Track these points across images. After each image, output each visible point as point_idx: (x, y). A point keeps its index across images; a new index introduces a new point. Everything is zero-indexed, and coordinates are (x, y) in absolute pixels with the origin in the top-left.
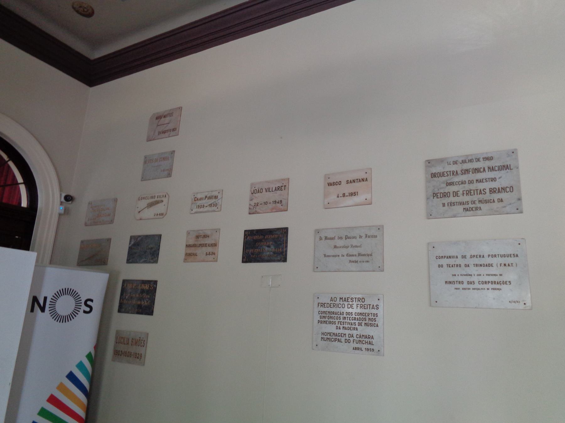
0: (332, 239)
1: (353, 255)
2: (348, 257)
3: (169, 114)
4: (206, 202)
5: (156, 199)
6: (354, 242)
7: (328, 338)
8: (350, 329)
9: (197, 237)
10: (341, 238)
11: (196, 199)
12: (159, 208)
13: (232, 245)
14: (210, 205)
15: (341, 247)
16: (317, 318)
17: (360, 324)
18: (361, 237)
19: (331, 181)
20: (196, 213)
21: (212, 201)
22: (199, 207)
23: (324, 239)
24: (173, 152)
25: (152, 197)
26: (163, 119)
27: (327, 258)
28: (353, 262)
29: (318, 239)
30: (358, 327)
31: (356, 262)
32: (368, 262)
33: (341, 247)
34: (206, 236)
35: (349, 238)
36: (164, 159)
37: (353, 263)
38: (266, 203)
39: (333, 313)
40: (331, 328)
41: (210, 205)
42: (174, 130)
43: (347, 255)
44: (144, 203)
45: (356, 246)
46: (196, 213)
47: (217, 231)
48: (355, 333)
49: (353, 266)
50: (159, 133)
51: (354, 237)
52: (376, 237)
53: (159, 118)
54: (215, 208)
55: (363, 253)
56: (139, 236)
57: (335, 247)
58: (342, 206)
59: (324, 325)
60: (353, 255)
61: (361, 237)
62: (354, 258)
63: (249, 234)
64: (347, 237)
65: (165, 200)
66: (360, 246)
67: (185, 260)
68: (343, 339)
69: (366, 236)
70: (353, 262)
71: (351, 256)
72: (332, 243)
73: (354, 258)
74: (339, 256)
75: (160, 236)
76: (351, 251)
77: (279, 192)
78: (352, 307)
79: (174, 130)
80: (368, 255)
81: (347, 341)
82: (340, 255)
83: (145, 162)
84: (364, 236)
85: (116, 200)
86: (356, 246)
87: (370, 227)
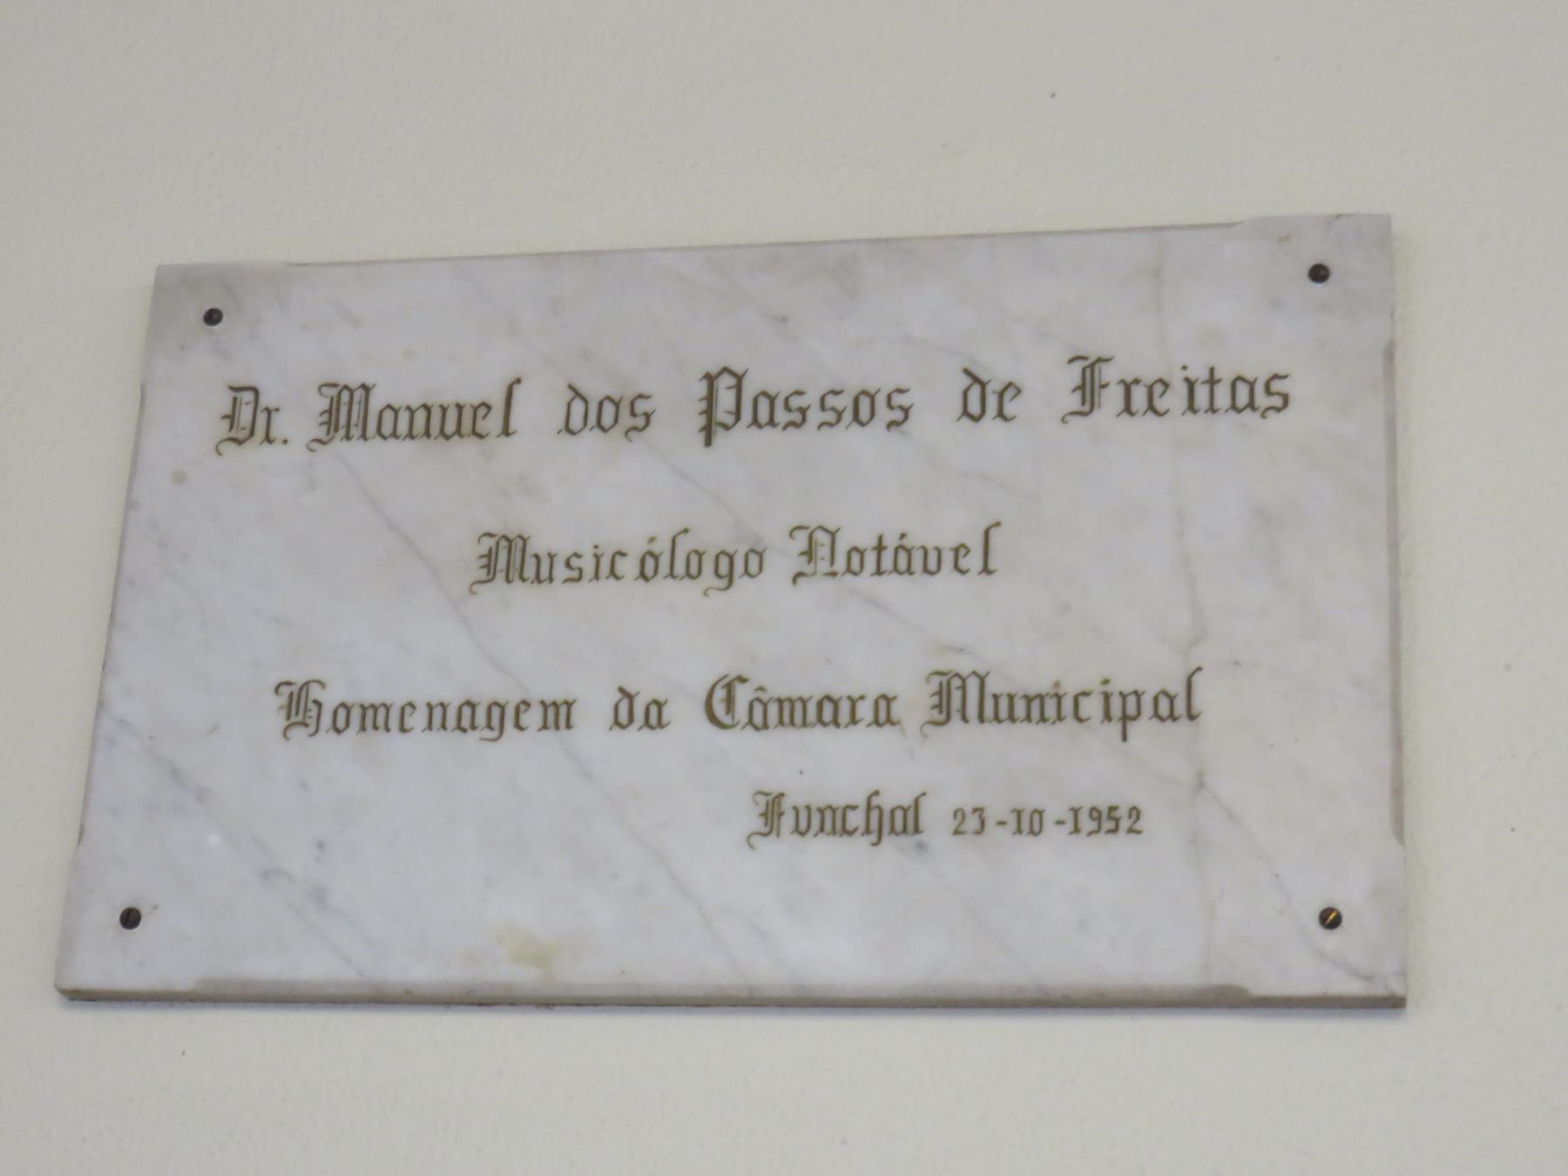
0: (452, 422)
1: (831, 712)
2: (740, 743)
6: (864, 480)
10: (619, 414)
15: (607, 566)
18: (985, 398)
23: (299, 420)
27: (334, 755)
28: (830, 821)
29: (193, 416)
31: (896, 822)
32: (1109, 820)
33: (607, 566)
35: (778, 411)
37: (824, 852)
43: (723, 703)
45: (901, 557)
49: (835, 909)
51: (861, 408)
52: (1261, 396)
55: (1024, 668)
57: (508, 559)
60: (831, 712)
61: (985, 398)
62: (840, 764)
64: (726, 404)
66: (978, 556)
69: (1089, 390)
70: (830, 821)
71: (791, 712)
72: (452, 494)
73: (840, 764)
74: (559, 714)
76: (795, 630)
80: (1123, 711)
82: (595, 706)
84: (1049, 384)
86: (901, 557)
87: (1160, 255)
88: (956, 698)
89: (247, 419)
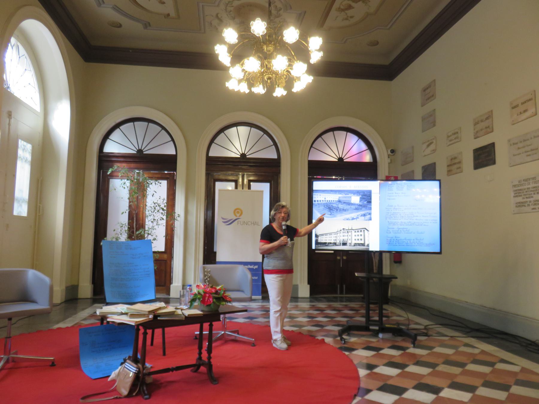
0: (517, 143)
3: (429, 86)
4: (453, 137)
6: (528, 143)
7: (520, 205)
8: (529, 198)
9: (452, 159)
10: (521, 142)
11: (448, 137)
12: (432, 147)
13: (468, 160)
14: (455, 139)
16: (512, 194)
17: (534, 194)
19: (514, 105)
20: (449, 145)
21: (456, 135)
22: (450, 141)
30: (534, 196)
34: (455, 158)
36: (431, 116)
38: (482, 130)
39: (520, 190)
40: (520, 199)
41: (455, 139)
42: (433, 96)
44: (425, 146)
45: (530, 145)
46: (449, 145)
47: (461, 153)
48: (532, 199)
49: (529, 159)
50: (427, 100)
51: (528, 140)
53: (425, 90)
54: (457, 140)
56: (425, 166)
58: (520, 120)
59: (516, 198)
61: (531, 138)
62: (528, 153)
63: (476, 151)
64: (525, 141)
65: (434, 141)
67: (448, 175)
68: (526, 205)
73: (528, 153)
75: (435, 163)
77: (487, 121)
78: (529, 184)
79: (433, 96)
81: (529, 205)
85: (413, 147)
88: (532, 150)
89: (511, 145)
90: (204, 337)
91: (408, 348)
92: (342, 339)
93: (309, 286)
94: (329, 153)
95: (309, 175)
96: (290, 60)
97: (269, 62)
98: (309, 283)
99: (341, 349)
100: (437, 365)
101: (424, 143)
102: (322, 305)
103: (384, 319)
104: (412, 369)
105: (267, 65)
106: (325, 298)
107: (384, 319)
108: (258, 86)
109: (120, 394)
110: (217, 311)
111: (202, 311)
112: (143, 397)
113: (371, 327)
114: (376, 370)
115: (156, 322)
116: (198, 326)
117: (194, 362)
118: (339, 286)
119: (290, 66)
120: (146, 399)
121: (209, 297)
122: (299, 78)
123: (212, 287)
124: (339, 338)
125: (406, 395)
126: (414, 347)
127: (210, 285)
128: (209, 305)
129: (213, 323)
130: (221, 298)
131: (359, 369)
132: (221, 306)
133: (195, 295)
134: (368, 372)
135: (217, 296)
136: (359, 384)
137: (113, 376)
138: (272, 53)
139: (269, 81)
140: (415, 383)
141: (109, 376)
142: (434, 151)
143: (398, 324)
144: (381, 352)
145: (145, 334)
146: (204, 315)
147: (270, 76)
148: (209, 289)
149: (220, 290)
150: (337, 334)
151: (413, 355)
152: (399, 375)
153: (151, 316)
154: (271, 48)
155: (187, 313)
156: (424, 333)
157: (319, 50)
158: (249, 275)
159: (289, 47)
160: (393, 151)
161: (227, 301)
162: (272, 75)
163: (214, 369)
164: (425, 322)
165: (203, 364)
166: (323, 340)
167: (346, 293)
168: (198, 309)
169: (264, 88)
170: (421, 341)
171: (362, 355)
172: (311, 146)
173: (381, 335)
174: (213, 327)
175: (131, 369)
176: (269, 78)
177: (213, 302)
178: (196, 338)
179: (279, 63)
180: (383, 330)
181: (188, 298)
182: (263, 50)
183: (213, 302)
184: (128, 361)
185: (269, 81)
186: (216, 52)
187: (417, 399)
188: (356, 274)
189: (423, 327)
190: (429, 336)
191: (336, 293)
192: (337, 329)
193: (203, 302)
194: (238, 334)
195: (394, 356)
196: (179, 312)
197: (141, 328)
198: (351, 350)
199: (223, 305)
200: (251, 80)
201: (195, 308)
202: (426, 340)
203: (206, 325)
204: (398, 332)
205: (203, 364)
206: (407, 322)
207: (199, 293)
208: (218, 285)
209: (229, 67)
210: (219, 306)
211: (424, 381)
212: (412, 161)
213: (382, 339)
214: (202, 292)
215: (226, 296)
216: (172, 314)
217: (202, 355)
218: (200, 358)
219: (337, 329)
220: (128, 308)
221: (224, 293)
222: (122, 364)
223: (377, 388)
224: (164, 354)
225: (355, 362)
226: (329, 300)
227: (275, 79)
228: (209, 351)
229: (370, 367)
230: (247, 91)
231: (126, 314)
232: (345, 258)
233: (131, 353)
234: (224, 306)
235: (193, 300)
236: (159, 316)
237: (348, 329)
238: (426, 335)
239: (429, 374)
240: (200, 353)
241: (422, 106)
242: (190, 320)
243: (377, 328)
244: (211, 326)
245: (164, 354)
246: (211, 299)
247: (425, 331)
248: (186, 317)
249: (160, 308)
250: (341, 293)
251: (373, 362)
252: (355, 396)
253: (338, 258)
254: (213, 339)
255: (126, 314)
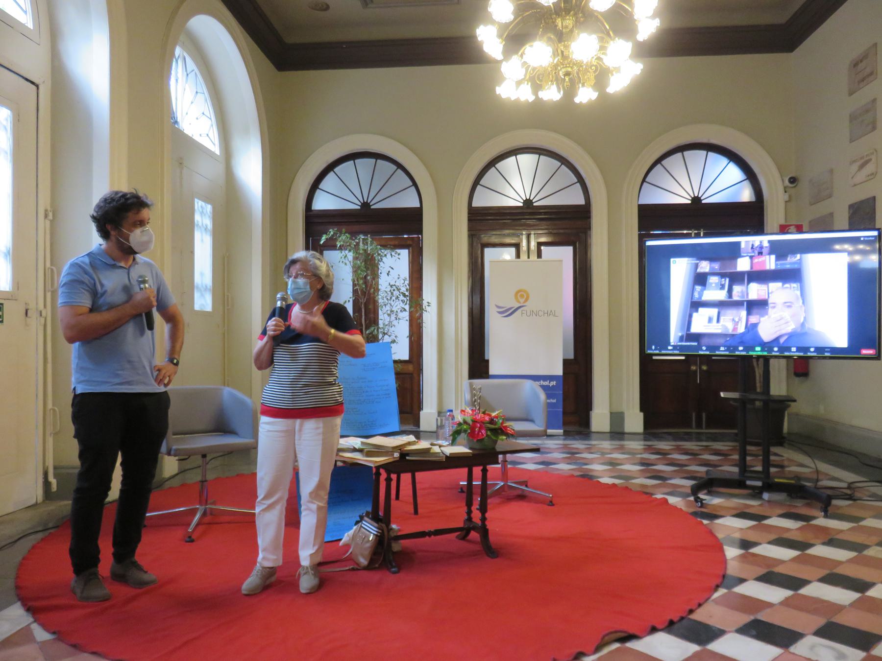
5: (866, 159)
12: (870, 168)
24: (874, 100)
25: (861, 158)
26: (860, 65)
36: (867, 111)
42: (871, 74)
44: (855, 167)
53: (856, 65)
65: (873, 158)
75: (874, 198)
79: (871, 74)
83: (851, 121)
85: (831, 171)
90: (474, 490)
91: (814, 518)
92: (697, 499)
93: (642, 414)
94: (675, 188)
95: (639, 230)
96: (601, 40)
97: (567, 47)
98: (641, 410)
99: (695, 514)
100: (867, 547)
101: (854, 161)
102: (664, 445)
103: (773, 470)
104: (820, 550)
105: (562, 52)
106: (669, 434)
107: (773, 470)
108: (549, 88)
109: (358, 564)
110: (494, 449)
111: (470, 449)
112: (389, 569)
113: (749, 483)
114: (754, 550)
115: (406, 463)
116: (465, 471)
117: (461, 525)
118: (694, 415)
119: (602, 48)
120: (394, 573)
121: (481, 428)
122: (618, 69)
123: (484, 413)
124: (692, 498)
125: (805, 591)
126: (826, 516)
127: (482, 410)
128: (483, 439)
129: (489, 467)
130: (501, 431)
131: (725, 548)
132: (499, 441)
133: (460, 424)
134: (741, 552)
135: (493, 426)
136: (726, 568)
137: (346, 538)
138: (572, 31)
139: (567, 79)
140: (824, 572)
141: (340, 540)
142: (873, 175)
143: (798, 477)
144: (766, 522)
145: (389, 480)
146: (474, 455)
147: (569, 69)
148: (480, 416)
149: (496, 417)
150: (689, 491)
151: (824, 530)
152: (794, 560)
153: (397, 455)
154: (569, 22)
155: (450, 450)
156: (847, 494)
157: (654, 17)
158: (542, 396)
159: (600, 17)
160: (793, 180)
161: (508, 435)
162: (572, 68)
163: (492, 538)
164: (849, 477)
165: (474, 528)
166: (666, 501)
167: (708, 427)
168: (465, 446)
169: (559, 91)
170: (838, 507)
171: (731, 526)
172: (644, 181)
173: (766, 496)
174: (489, 475)
175: (370, 530)
176: (567, 74)
177: (487, 435)
178: (462, 491)
179: (584, 46)
180: (770, 486)
181: (448, 430)
182: (556, 26)
183: (487, 435)
184: (366, 518)
185: (567, 79)
186: (479, 39)
187: (826, 598)
188: (722, 395)
189: (845, 485)
190: (855, 500)
191: (690, 427)
192: (690, 483)
193: (472, 435)
194: (526, 486)
195: (788, 530)
196: (436, 449)
197: (382, 471)
198: (713, 517)
199: (503, 440)
200: (537, 80)
201: (459, 445)
202: (849, 505)
203: (477, 471)
204: (797, 490)
205: (474, 528)
206: (815, 477)
207: (465, 422)
208: (494, 411)
209: (501, 62)
210: (495, 442)
211: (840, 570)
212: (830, 196)
213: (769, 501)
214: (469, 420)
215: (506, 427)
216: (426, 451)
217: (472, 515)
218: (470, 519)
219: (690, 483)
220: (362, 443)
221: (502, 423)
222: (357, 523)
223: (756, 576)
224: (416, 512)
225: (720, 536)
226: (676, 437)
227: (578, 74)
228: (483, 509)
229: (746, 545)
230: (531, 98)
231: (360, 451)
232: (704, 368)
233: (370, 509)
234: (503, 443)
235: (456, 433)
236: (408, 455)
237: (709, 484)
238: (850, 498)
239: (850, 561)
240: (469, 512)
241: (851, 93)
242: (453, 461)
243: (759, 484)
244: (485, 471)
245: (416, 512)
246: (483, 432)
247: (848, 492)
248: (447, 456)
249: (409, 444)
250: (699, 426)
251: (751, 537)
252: (717, 587)
253: (693, 368)
254: (489, 492)
255: (360, 451)
